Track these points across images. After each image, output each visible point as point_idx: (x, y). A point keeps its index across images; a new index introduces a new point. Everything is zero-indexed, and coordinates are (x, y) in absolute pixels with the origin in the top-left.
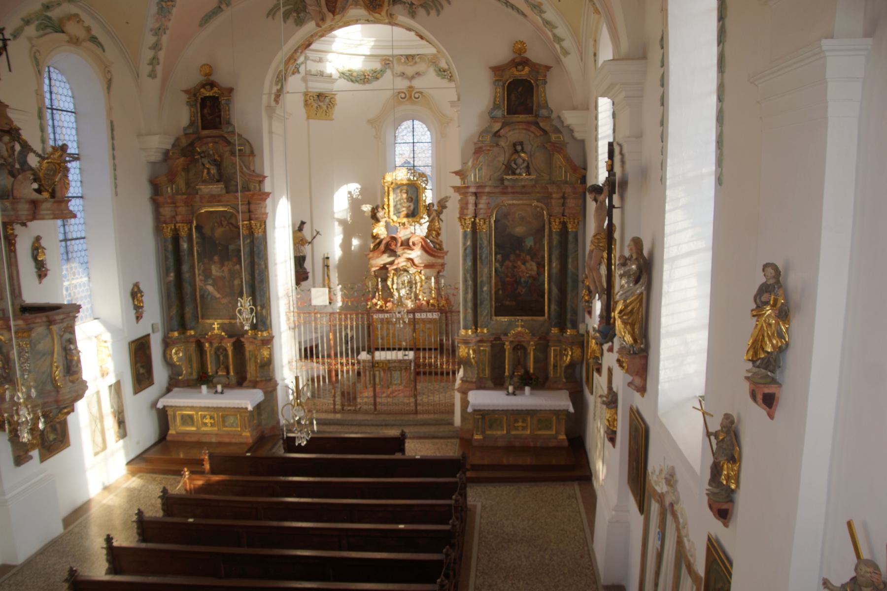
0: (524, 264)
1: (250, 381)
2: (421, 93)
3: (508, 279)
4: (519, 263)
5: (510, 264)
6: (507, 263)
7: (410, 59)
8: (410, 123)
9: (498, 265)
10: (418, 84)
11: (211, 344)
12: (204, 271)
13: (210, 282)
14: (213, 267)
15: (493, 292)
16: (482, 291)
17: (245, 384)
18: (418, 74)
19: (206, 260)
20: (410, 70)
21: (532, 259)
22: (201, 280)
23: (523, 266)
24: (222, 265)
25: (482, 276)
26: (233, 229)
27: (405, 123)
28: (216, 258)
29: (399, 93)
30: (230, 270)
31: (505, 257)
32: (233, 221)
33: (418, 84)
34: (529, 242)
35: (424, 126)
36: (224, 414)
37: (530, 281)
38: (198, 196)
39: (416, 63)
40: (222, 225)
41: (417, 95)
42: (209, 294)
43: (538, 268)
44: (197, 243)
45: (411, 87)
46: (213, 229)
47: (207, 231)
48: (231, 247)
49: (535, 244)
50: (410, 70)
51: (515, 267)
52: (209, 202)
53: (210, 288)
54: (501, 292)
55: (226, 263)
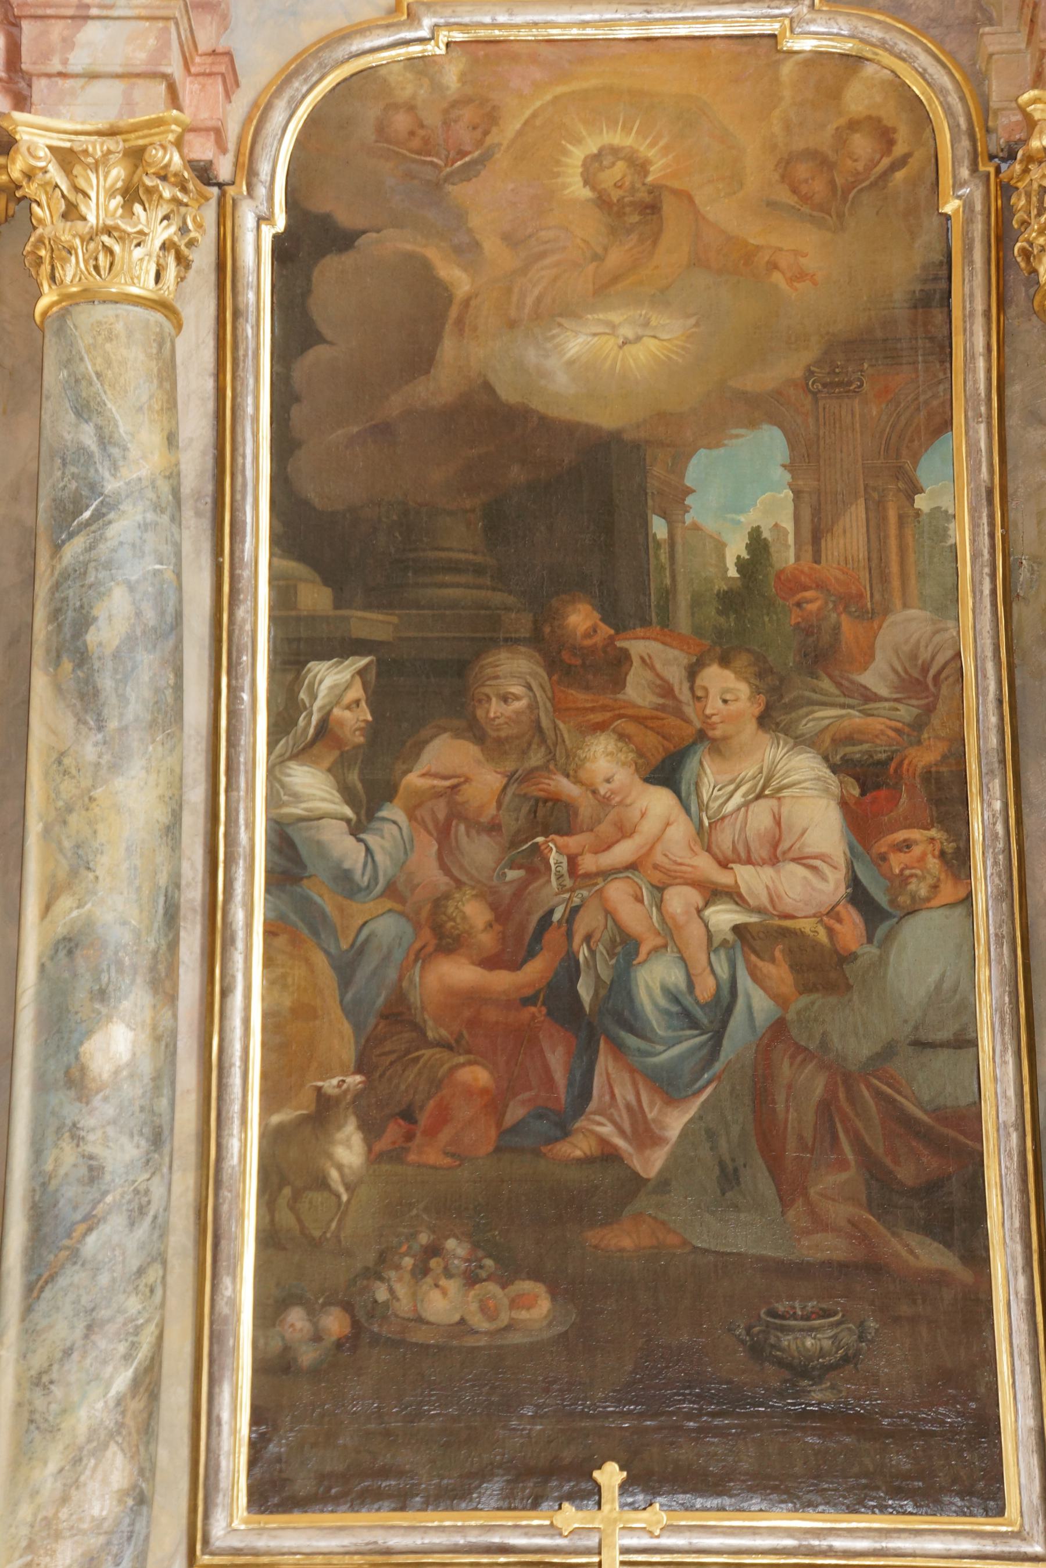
0: (666, 772)
3: (459, 973)
4: (605, 761)
5: (487, 784)
6: (445, 755)
9: (313, 786)
15: (245, 1148)
16: (68, 1078)
21: (765, 721)
23: (659, 801)
25: (75, 870)
31: (421, 691)
34: (737, 501)
37: (757, 1003)
43: (861, 823)
49: (815, 532)
51: (552, 816)
54: (348, 1150)
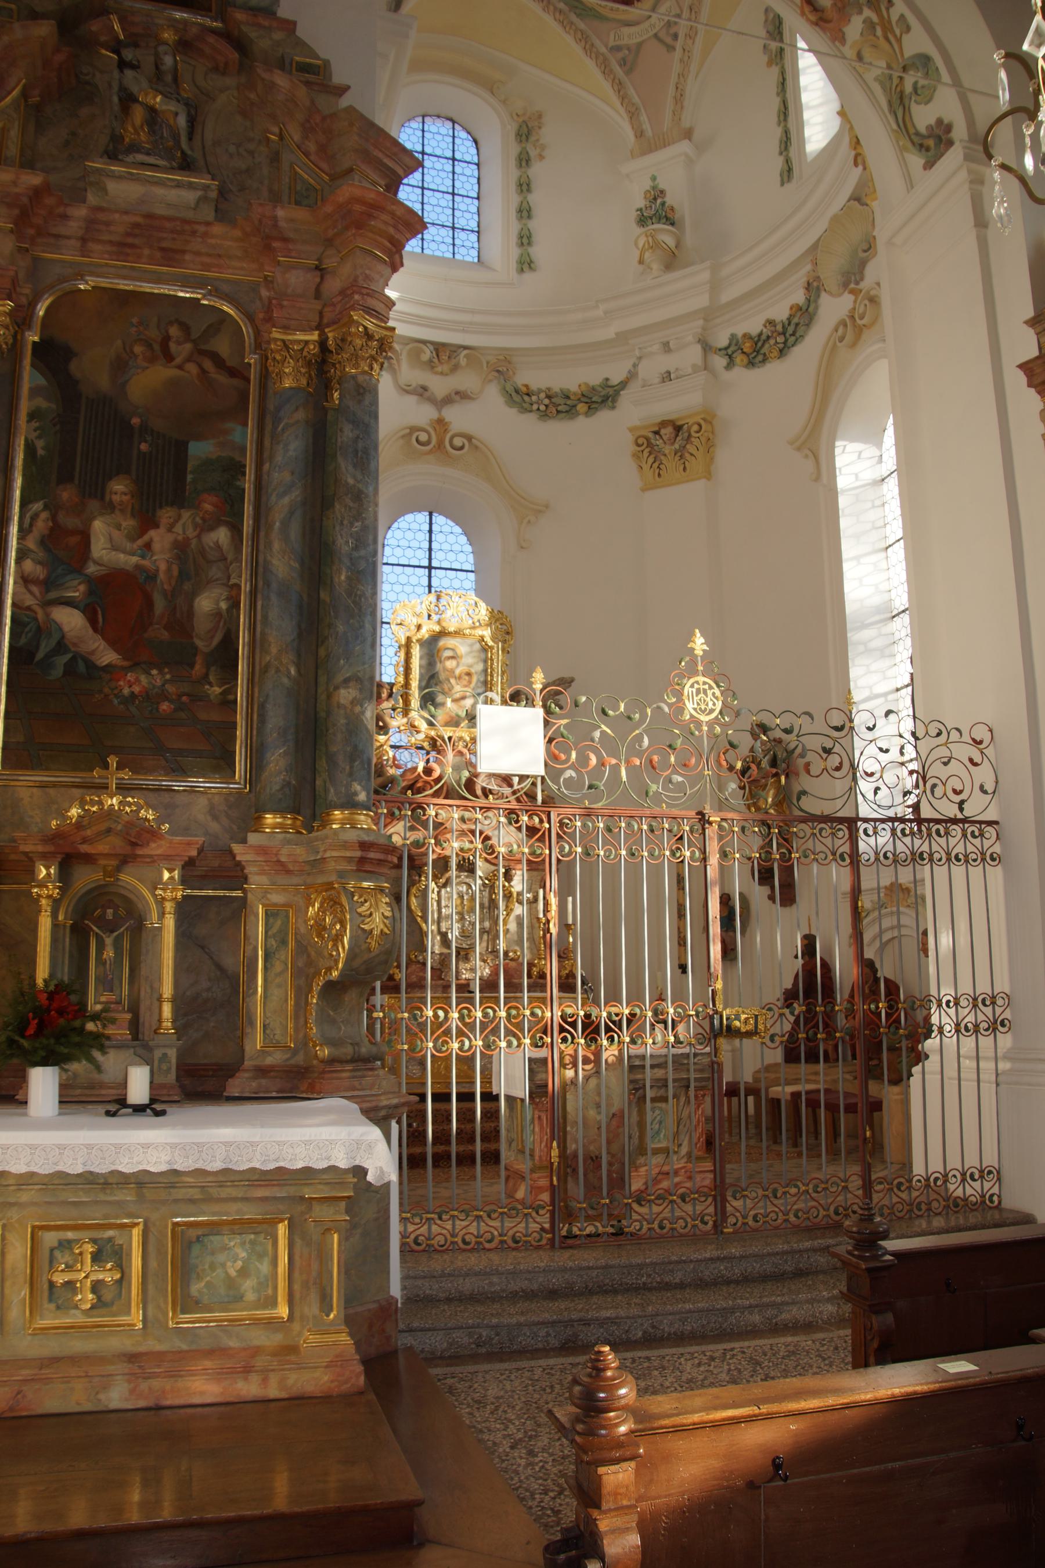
1: (262, 1071)
2: (469, 438)
7: (445, 358)
8: (422, 517)
10: (458, 418)
11: (65, 875)
12: (53, 539)
13: (76, 591)
14: (98, 525)
17: (234, 1087)
18: (462, 396)
19: (66, 494)
20: (440, 386)
22: (24, 580)
24: (147, 522)
26: (221, 378)
27: (409, 517)
28: (119, 488)
29: (413, 429)
30: (181, 548)
32: (222, 346)
33: (458, 418)
35: (458, 530)
36: (186, 1218)
38: (80, 212)
39: (455, 368)
40: (169, 358)
41: (458, 442)
42: (61, 646)
44: (32, 416)
45: (441, 423)
46: (120, 366)
47: (93, 369)
48: (200, 450)
50: (440, 386)
52: (123, 248)
53: (70, 621)
55: (166, 515)
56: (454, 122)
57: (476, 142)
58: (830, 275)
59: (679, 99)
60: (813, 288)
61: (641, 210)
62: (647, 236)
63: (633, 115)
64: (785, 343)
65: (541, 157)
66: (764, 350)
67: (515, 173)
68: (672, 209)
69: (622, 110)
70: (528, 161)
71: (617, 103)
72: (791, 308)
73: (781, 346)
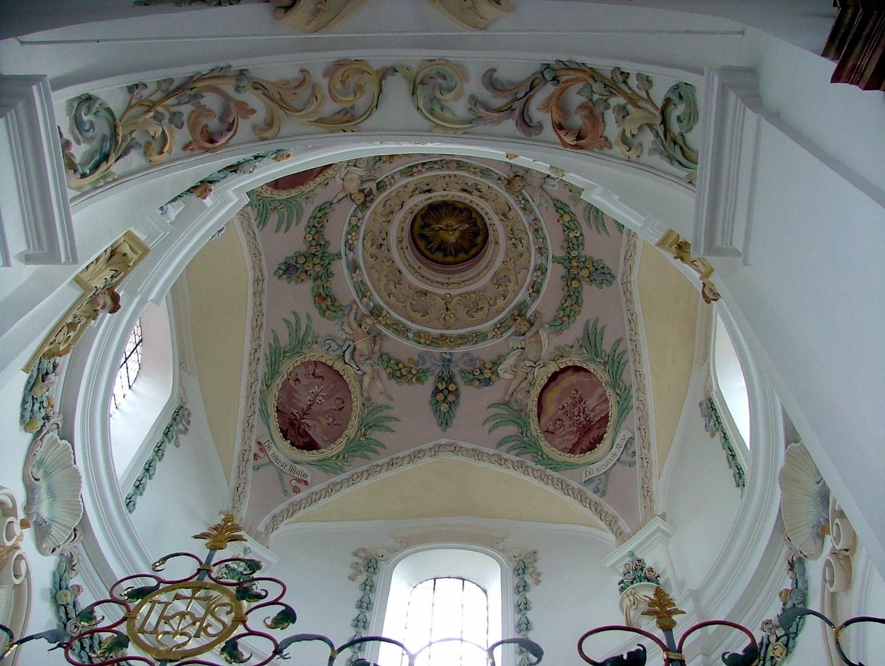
56: (463, 580)
57: (485, 592)
58: (803, 540)
59: (647, 493)
60: (796, 565)
61: (622, 581)
62: (628, 596)
63: (612, 523)
64: (787, 635)
65: (538, 582)
66: (770, 654)
67: (513, 598)
68: (651, 570)
69: (602, 524)
70: (525, 587)
71: (596, 519)
72: (780, 595)
73: (784, 639)
